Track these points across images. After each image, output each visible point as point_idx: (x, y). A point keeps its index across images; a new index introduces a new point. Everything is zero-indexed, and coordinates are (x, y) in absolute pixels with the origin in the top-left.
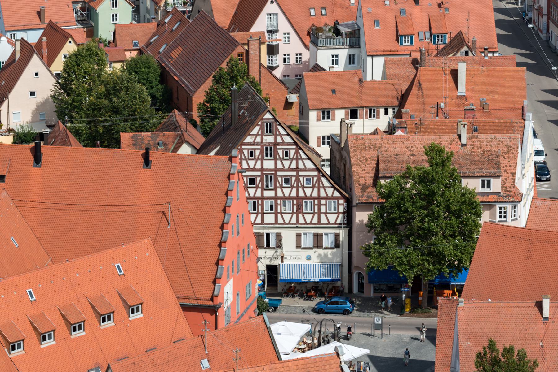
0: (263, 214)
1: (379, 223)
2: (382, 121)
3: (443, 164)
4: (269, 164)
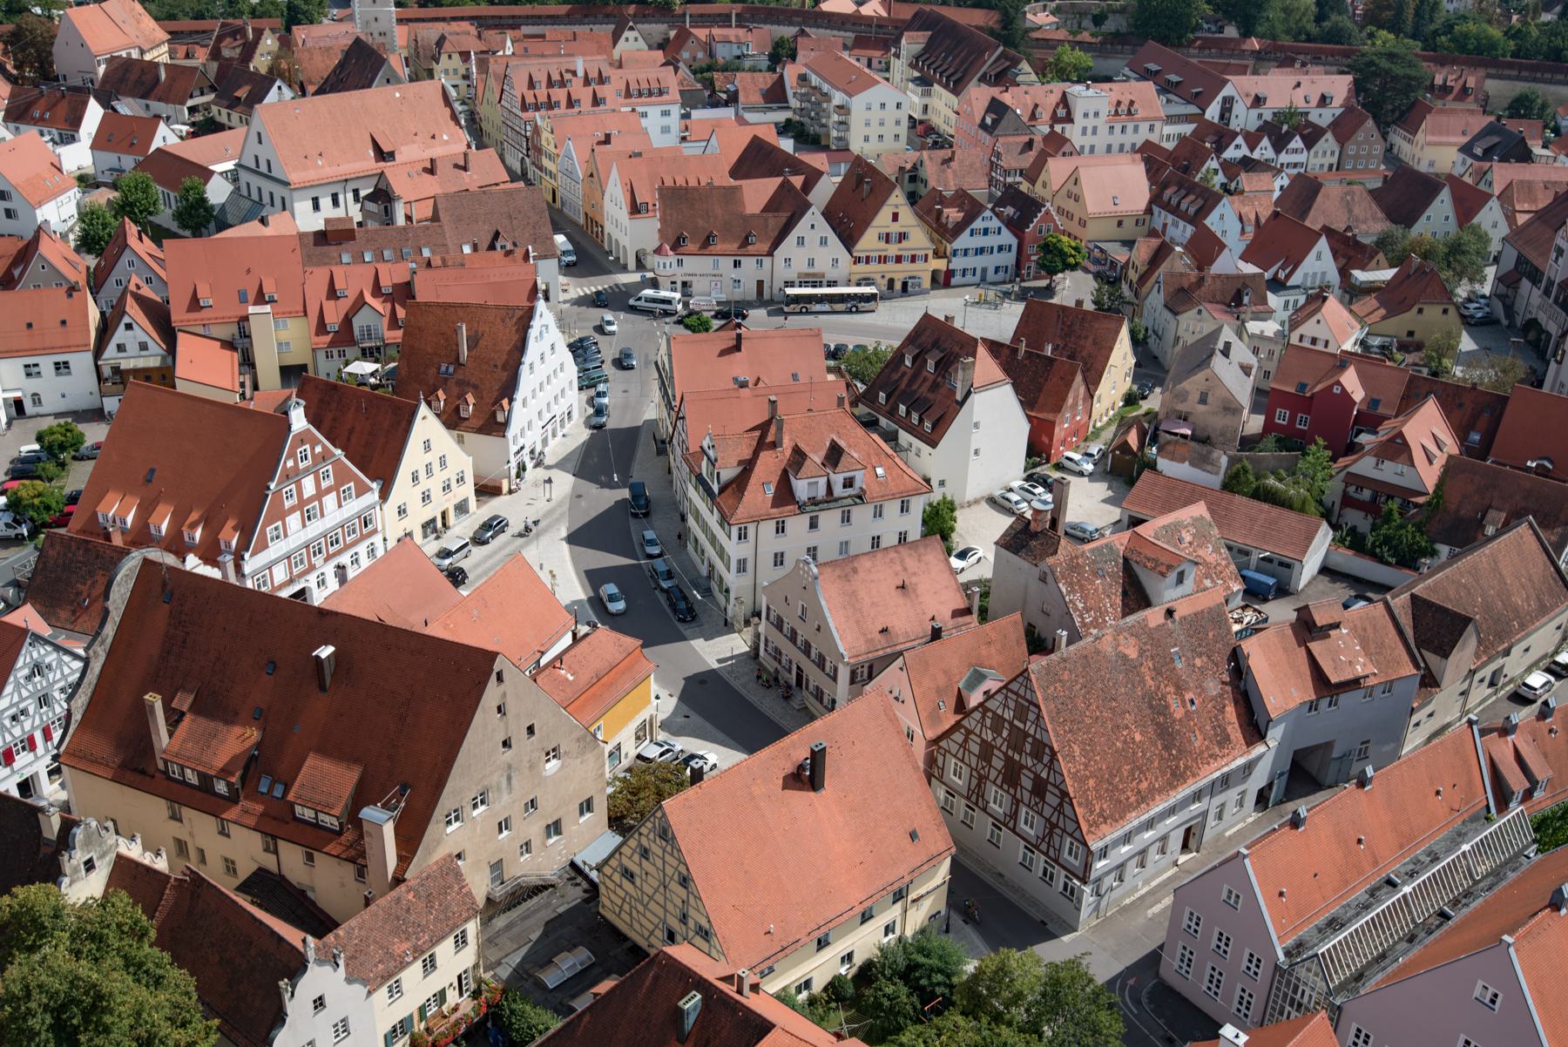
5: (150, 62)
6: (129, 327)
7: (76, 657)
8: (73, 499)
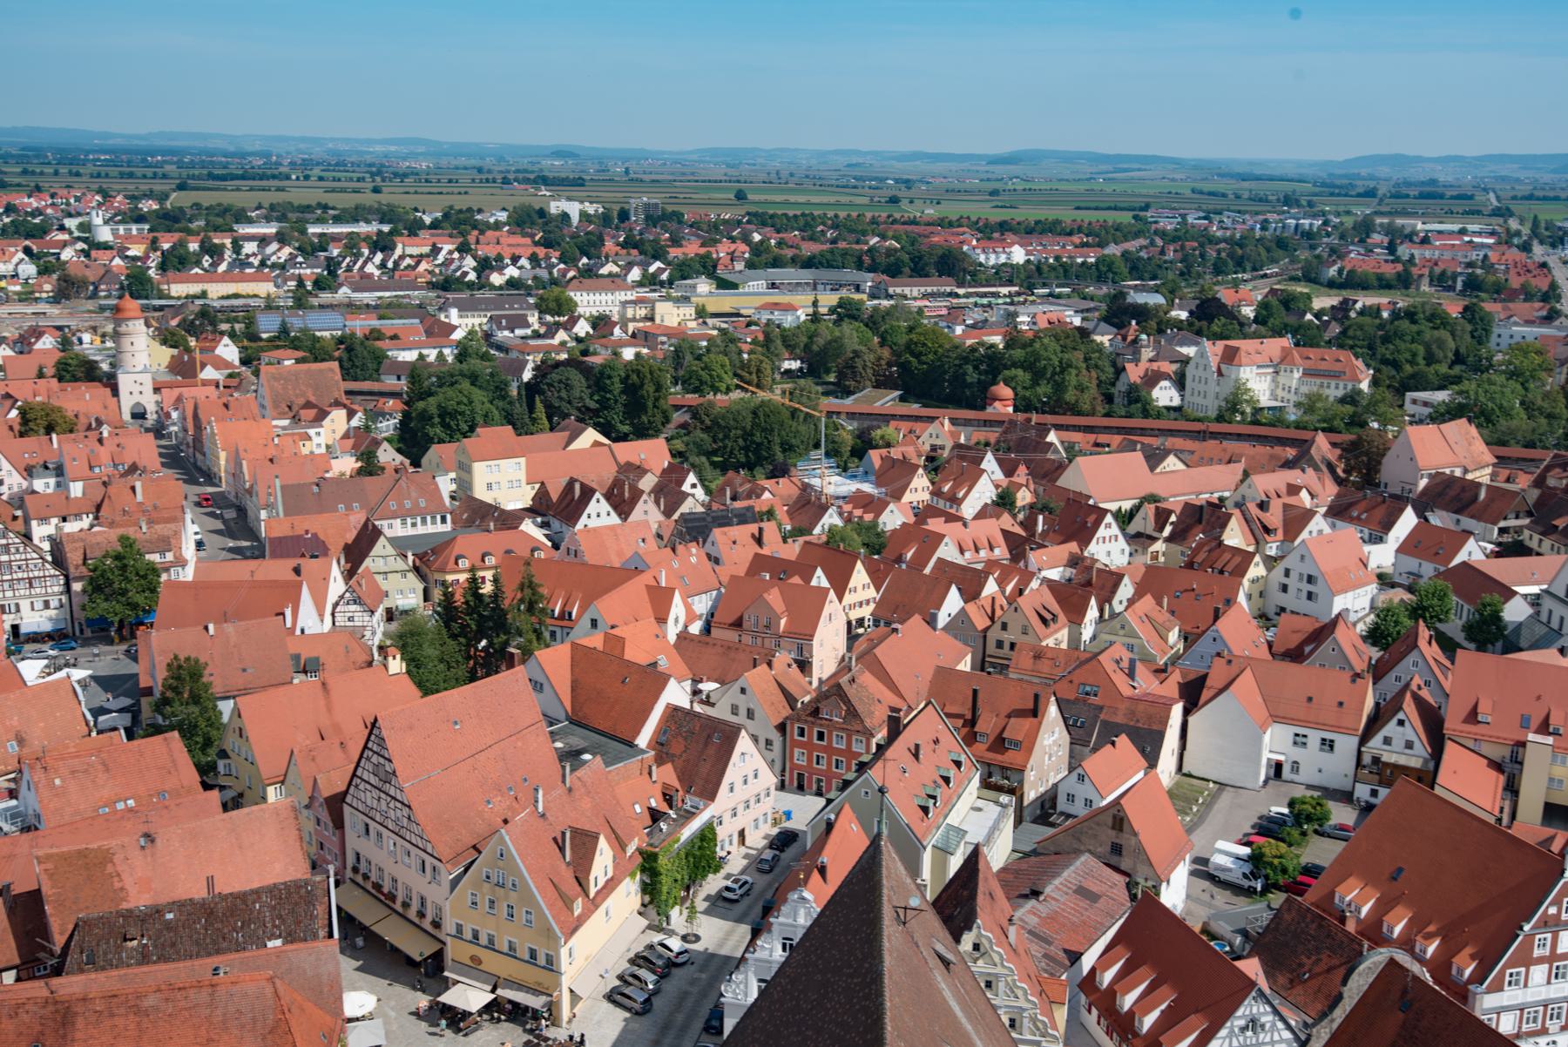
2: (86, 522)
5: (1472, 481)
6: (1401, 723)
7: (1289, 1027)
8: (1312, 871)
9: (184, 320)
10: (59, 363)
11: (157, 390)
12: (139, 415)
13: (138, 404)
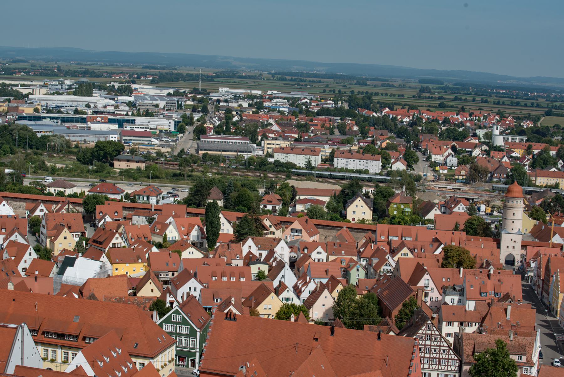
0: (424, 364)
1: (474, 371)
3: (503, 348)
4: (428, 343)
9: (545, 202)
10: (468, 222)
11: (523, 247)
12: (510, 262)
13: (511, 255)
